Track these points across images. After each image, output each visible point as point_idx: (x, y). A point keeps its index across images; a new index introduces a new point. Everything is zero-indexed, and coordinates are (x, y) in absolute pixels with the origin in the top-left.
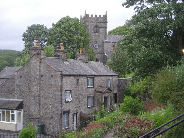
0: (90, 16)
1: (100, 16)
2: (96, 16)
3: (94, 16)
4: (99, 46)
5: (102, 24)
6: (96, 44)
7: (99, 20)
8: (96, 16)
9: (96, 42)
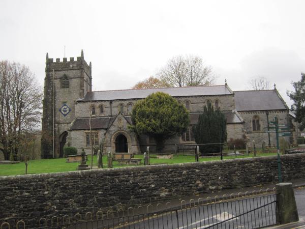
0: (55, 61)
1: (72, 59)
2: (65, 59)
3: (61, 60)
4: (70, 110)
5: (74, 71)
6: (65, 107)
7: (69, 65)
8: (65, 59)
9: (64, 103)
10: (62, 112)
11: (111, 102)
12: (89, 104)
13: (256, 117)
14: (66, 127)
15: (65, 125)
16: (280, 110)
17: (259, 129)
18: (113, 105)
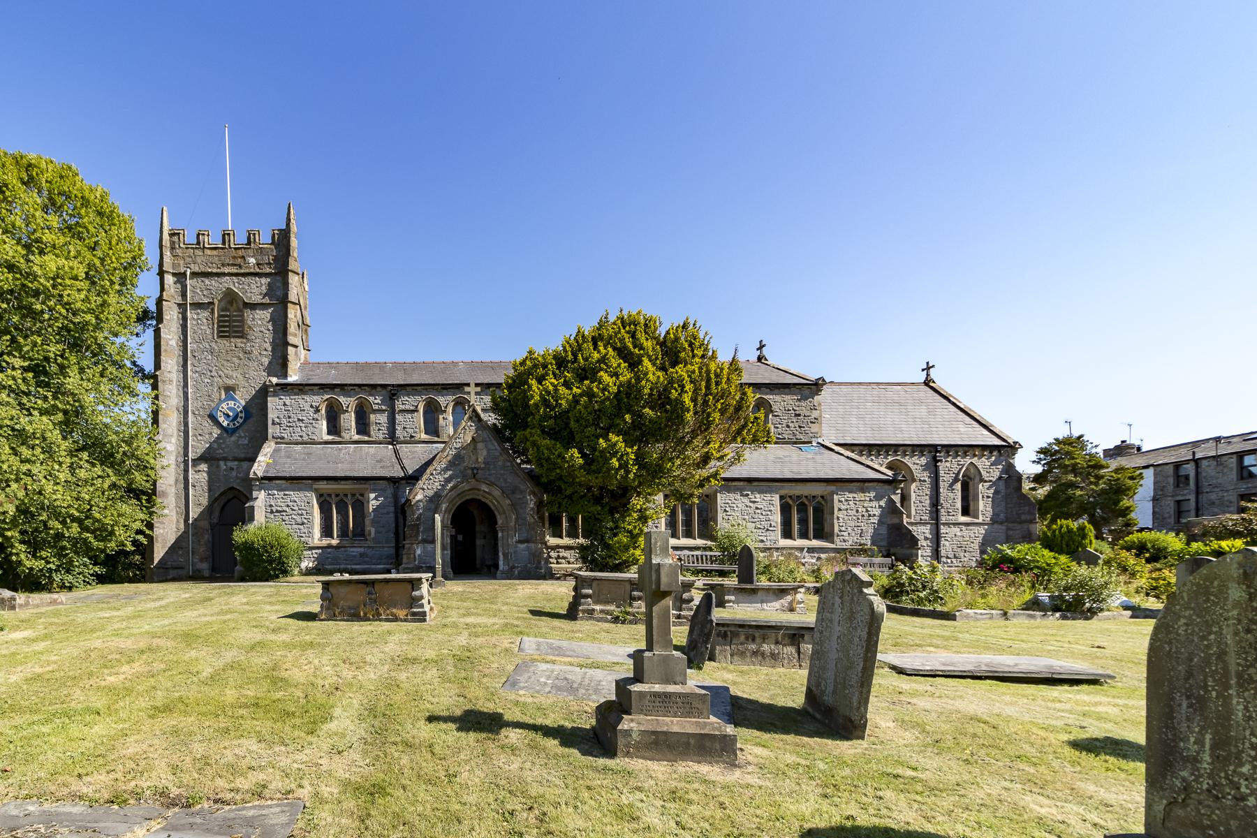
6: (231, 404)
10: (221, 419)
11: (393, 392)
12: (318, 400)
14: (234, 474)
15: (230, 464)
18: (399, 405)
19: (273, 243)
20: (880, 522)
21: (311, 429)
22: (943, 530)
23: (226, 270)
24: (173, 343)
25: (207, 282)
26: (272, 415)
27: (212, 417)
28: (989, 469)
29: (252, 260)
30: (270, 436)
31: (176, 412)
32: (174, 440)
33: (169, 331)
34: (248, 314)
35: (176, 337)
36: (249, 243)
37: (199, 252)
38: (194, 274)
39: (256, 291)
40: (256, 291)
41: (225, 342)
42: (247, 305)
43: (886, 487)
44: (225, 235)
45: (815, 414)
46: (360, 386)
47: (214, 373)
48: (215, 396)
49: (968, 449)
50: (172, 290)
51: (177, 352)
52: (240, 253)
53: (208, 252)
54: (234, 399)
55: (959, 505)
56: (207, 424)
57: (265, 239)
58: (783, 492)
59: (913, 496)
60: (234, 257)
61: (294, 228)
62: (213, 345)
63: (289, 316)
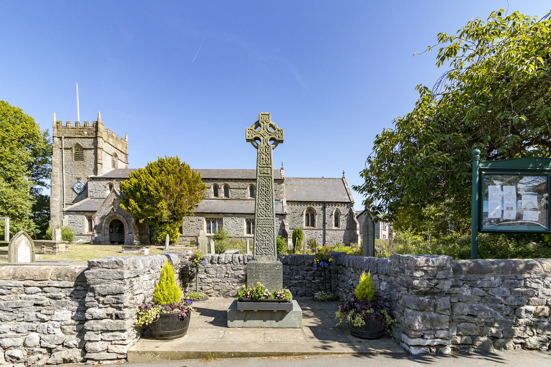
6: (79, 184)
10: (75, 190)
12: (105, 183)
13: (310, 210)
16: (342, 203)
17: (313, 225)
19: (93, 126)
20: (280, 229)
21: (103, 194)
22: (327, 232)
23: (77, 136)
24: (58, 162)
25: (70, 140)
26: (89, 189)
27: (73, 189)
28: (344, 210)
29: (86, 133)
30: (89, 196)
31: (59, 187)
32: (58, 197)
33: (56, 158)
34: (84, 151)
35: (59, 160)
36: (85, 126)
37: (67, 130)
38: (65, 138)
39: (88, 144)
40: (88, 144)
41: (76, 162)
42: (84, 149)
43: (281, 216)
44: (76, 123)
45: (282, 190)
46: (120, 178)
47: (73, 173)
48: (74, 181)
49: (336, 203)
50: (58, 143)
51: (60, 165)
52: (82, 130)
53: (70, 129)
54: (80, 182)
55: (333, 223)
56: (71, 191)
57: (90, 125)
58: (247, 218)
59: (316, 220)
60: (79, 131)
61: (100, 121)
62: (72, 163)
63: (98, 153)
